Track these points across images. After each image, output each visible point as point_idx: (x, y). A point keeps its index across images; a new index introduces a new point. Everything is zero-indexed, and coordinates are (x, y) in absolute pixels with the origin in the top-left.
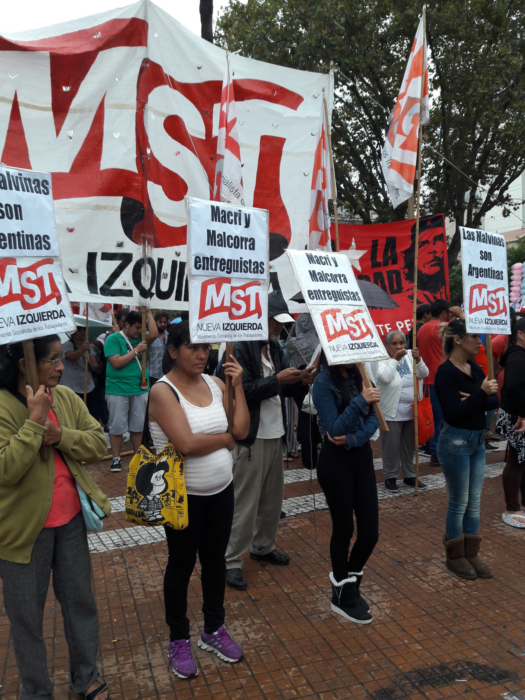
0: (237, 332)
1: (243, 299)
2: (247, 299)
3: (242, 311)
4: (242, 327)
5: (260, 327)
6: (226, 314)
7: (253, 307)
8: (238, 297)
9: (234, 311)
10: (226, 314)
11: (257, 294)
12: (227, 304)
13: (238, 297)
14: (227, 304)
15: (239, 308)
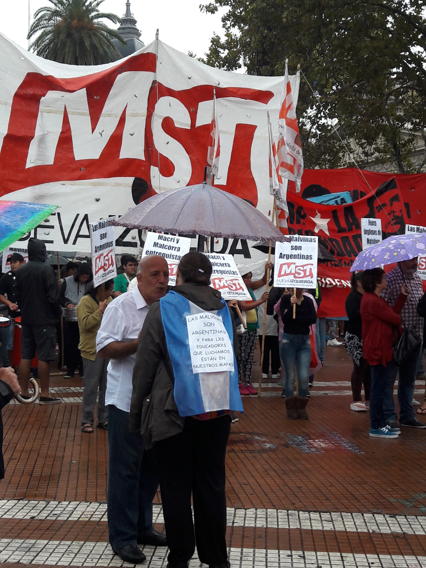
0: (298, 283)
1: (302, 270)
2: (305, 271)
3: (302, 275)
4: (301, 281)
5: (312, 282)
6: (293, 276)
7: (308, 274)
8: (299, 269)
9: (297, 275)
10: (293, 276)
11: (311, 269)
12: (293, 272)
13: (299, 269)
14: (293, 272)
15: (299, 274)
